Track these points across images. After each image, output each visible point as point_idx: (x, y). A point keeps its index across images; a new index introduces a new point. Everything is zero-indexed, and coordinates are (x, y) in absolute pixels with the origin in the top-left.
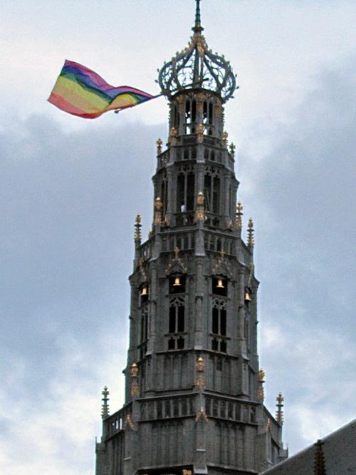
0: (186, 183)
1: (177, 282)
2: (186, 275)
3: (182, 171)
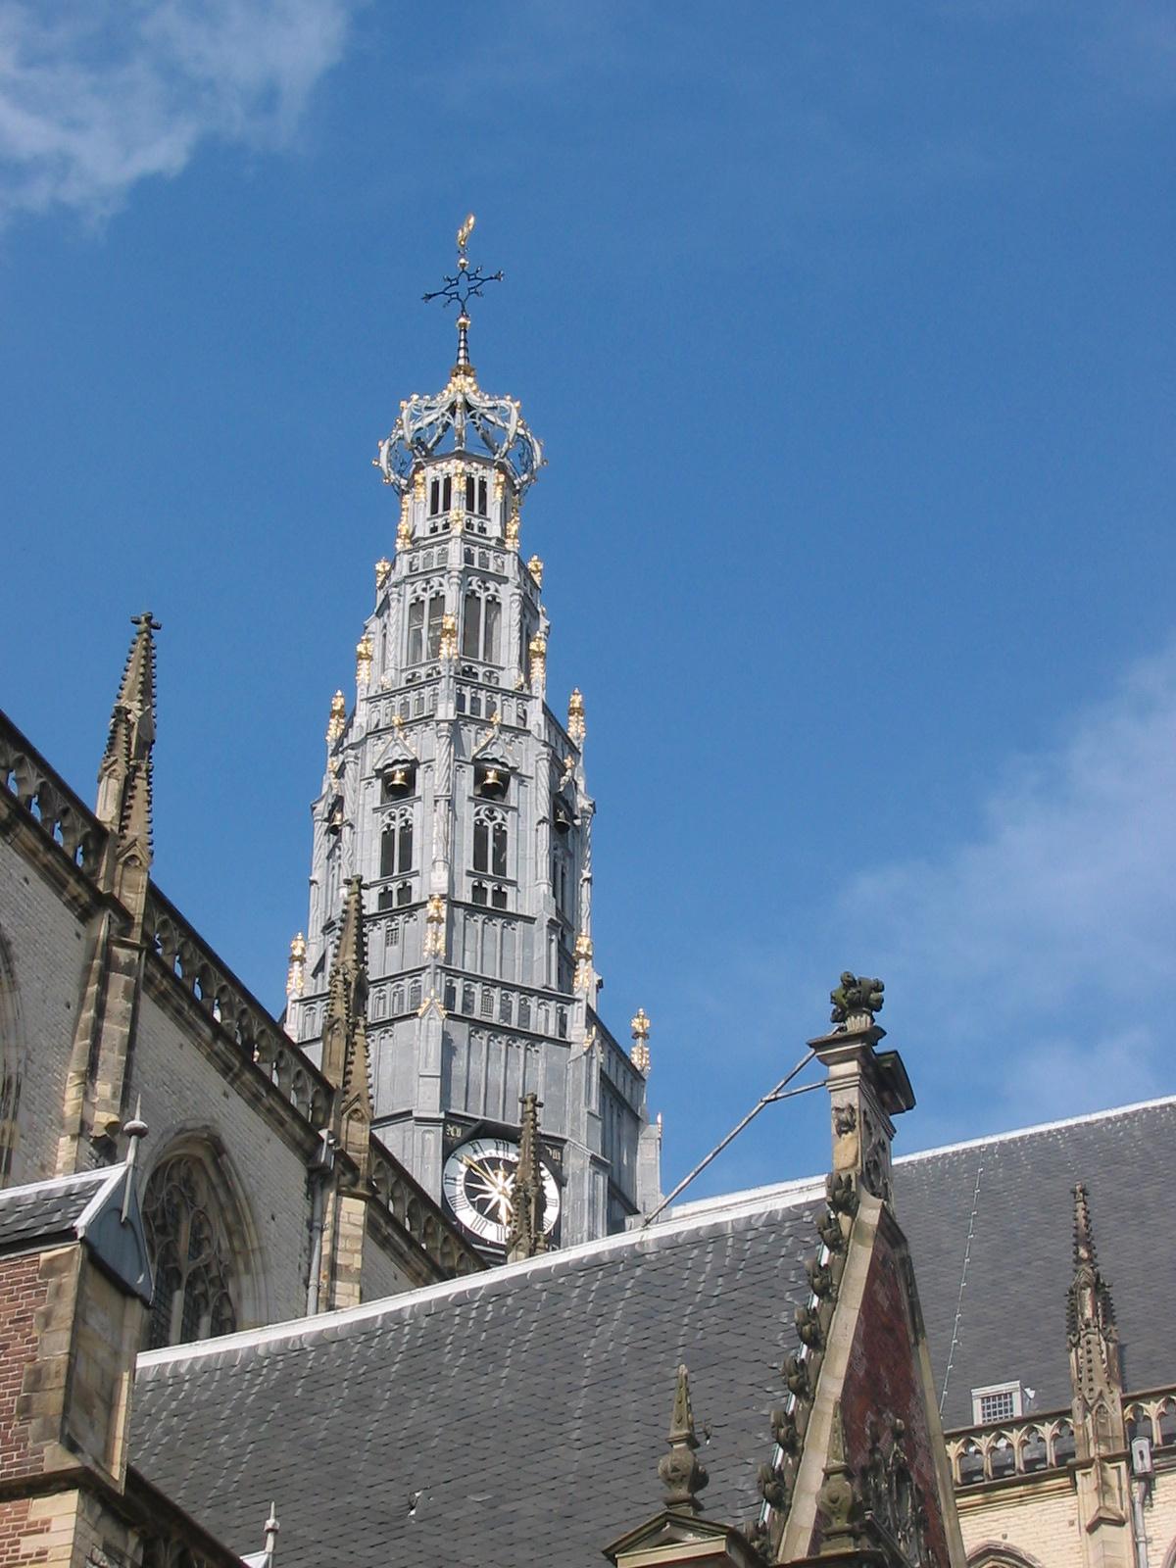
2: (513, 769)
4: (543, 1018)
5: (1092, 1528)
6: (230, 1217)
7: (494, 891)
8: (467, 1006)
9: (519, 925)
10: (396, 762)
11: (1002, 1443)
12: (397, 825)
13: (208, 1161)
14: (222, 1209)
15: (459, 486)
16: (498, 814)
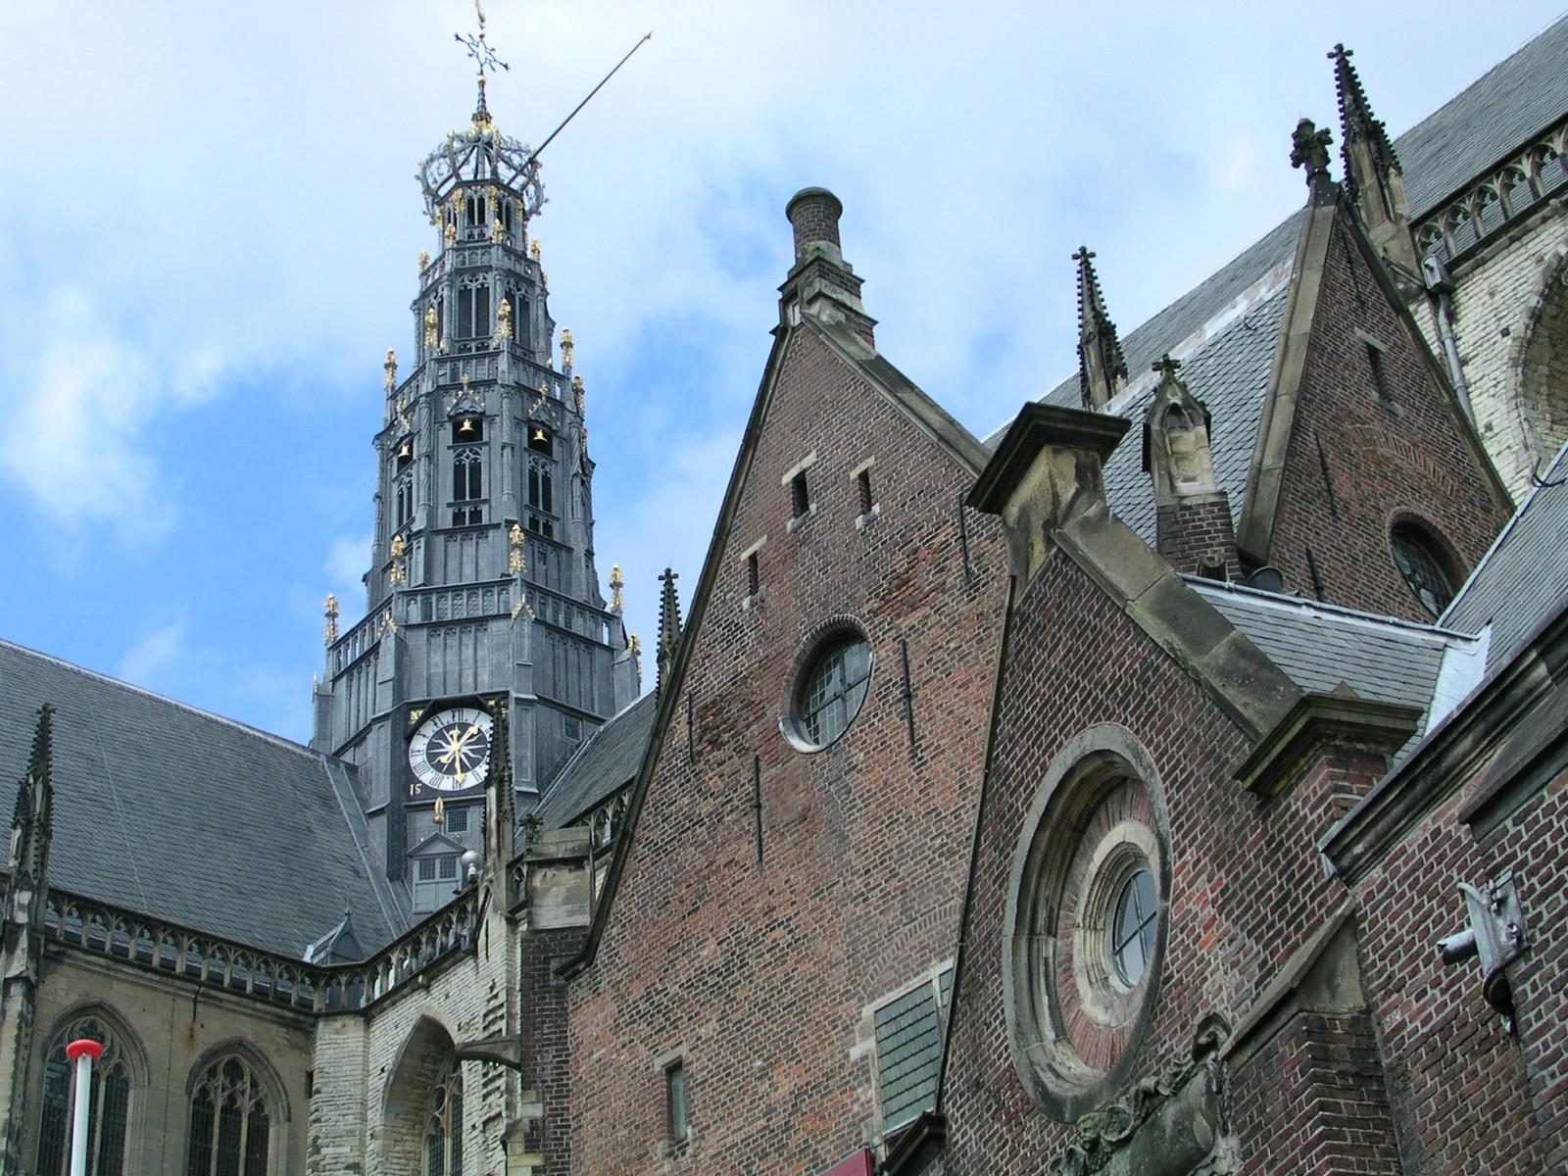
0: (471, 307)
1: (467, 426)
3: (467, 282)
7: (471, 513)
10: (402, 439)
15: (462, 208)
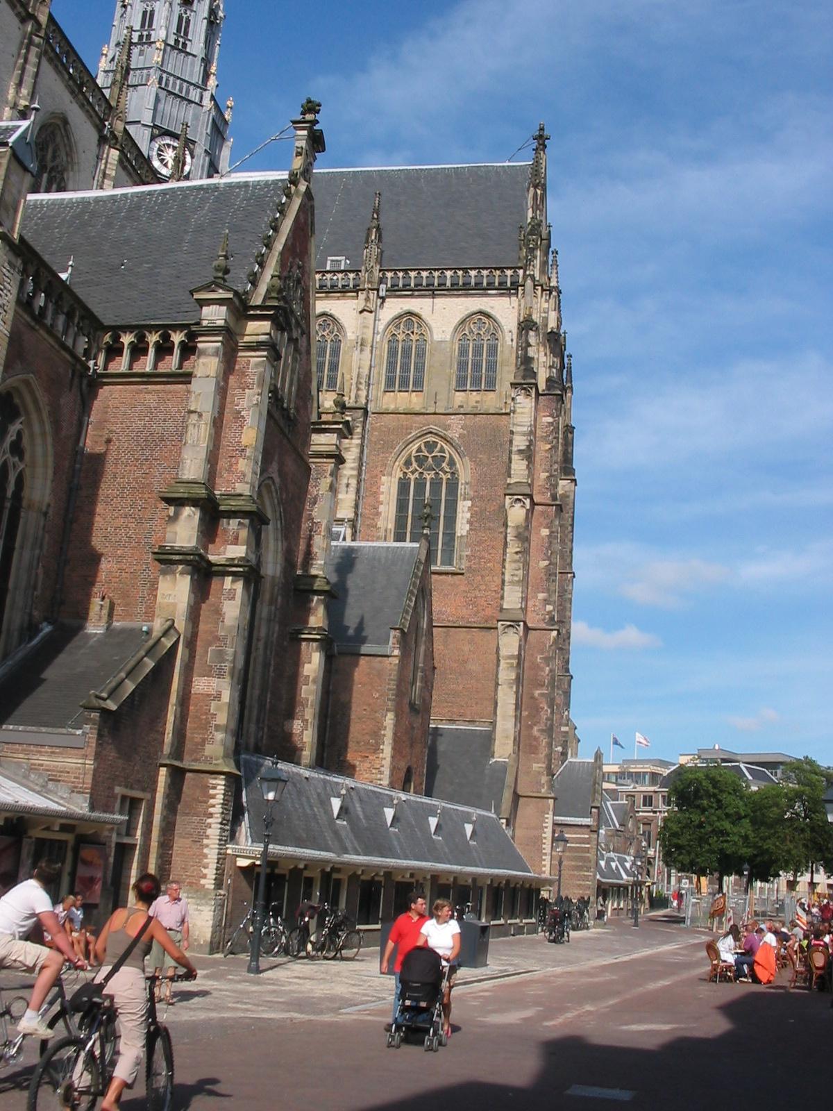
4: (194, 95)
5: (361, 312)
6: (68, 149)
8: (167, 85)
9: (190, 57)
11: (335, 278)
12: (149, 9)
13: (61, 126)
14: (65, 145)
16: (188, 12)
